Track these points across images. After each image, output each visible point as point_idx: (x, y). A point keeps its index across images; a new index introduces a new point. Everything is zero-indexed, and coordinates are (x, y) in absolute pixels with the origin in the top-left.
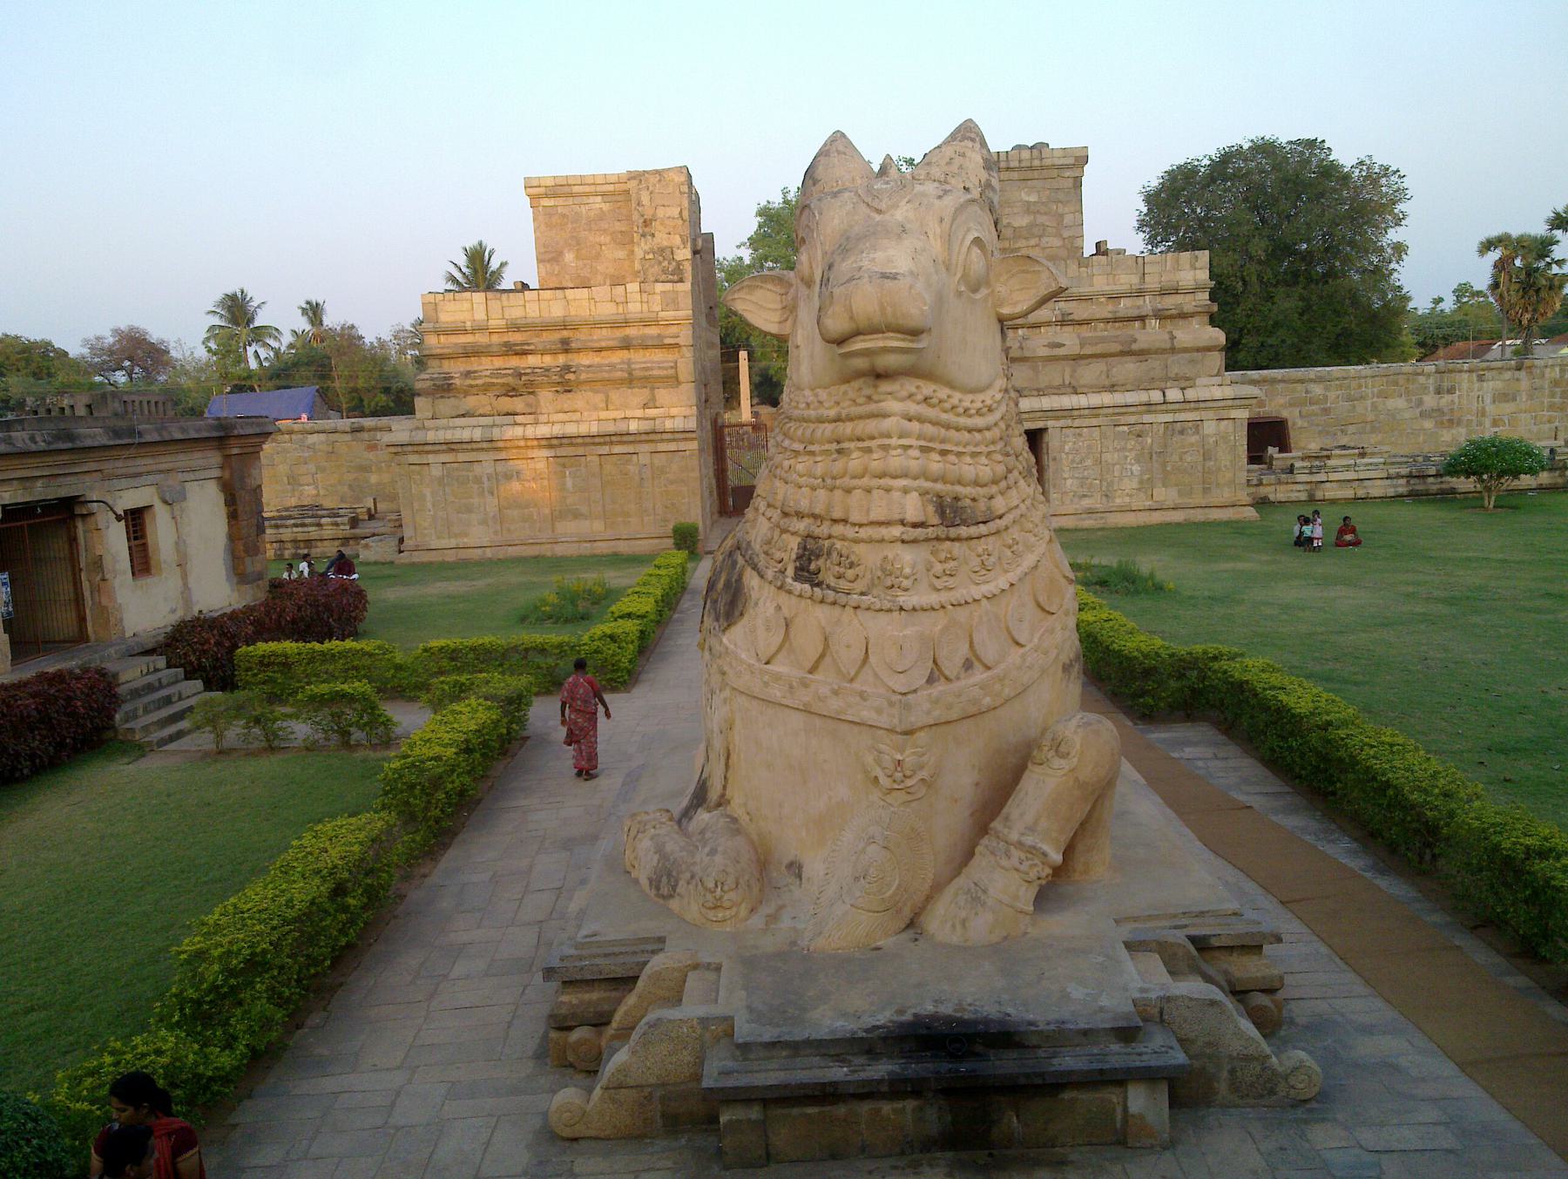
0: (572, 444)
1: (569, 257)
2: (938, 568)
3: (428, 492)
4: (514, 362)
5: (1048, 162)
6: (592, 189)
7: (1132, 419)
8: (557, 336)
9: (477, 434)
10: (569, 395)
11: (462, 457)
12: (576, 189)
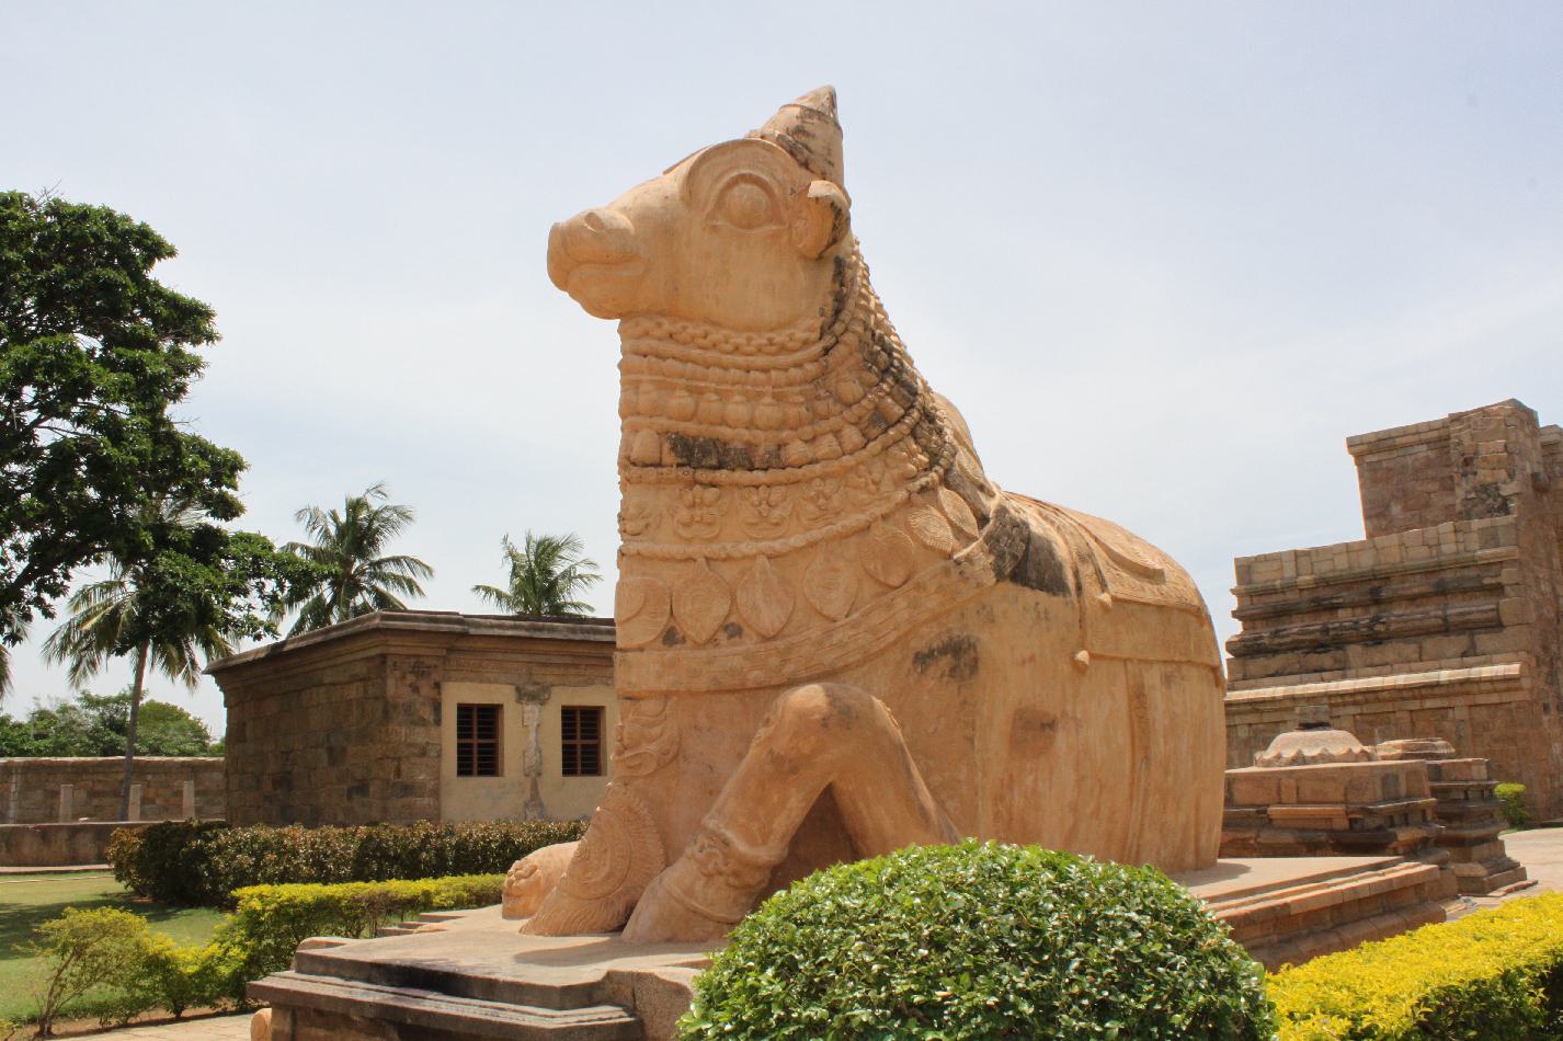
0: (1378, 700)
1: (1396, 509)
2: (684, 514)
4: (1325, 618)
6: (1416, 438)
8: (1367, 587)
9: (1278, 691)
10: (1380, 648)
11: (1267, 718)
12: (1398, 441)
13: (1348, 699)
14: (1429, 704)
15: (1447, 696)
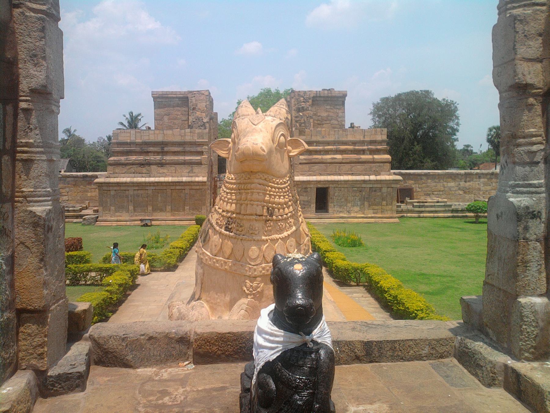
1: (166, 118)
3: (108, 200)
5: (334, 95)
6: (175, 96)
7: (358, 186)
9: (128, 180)
11: (122, 188)
13: (152, 184)
14: (177, 188)
15: (185, 185)
